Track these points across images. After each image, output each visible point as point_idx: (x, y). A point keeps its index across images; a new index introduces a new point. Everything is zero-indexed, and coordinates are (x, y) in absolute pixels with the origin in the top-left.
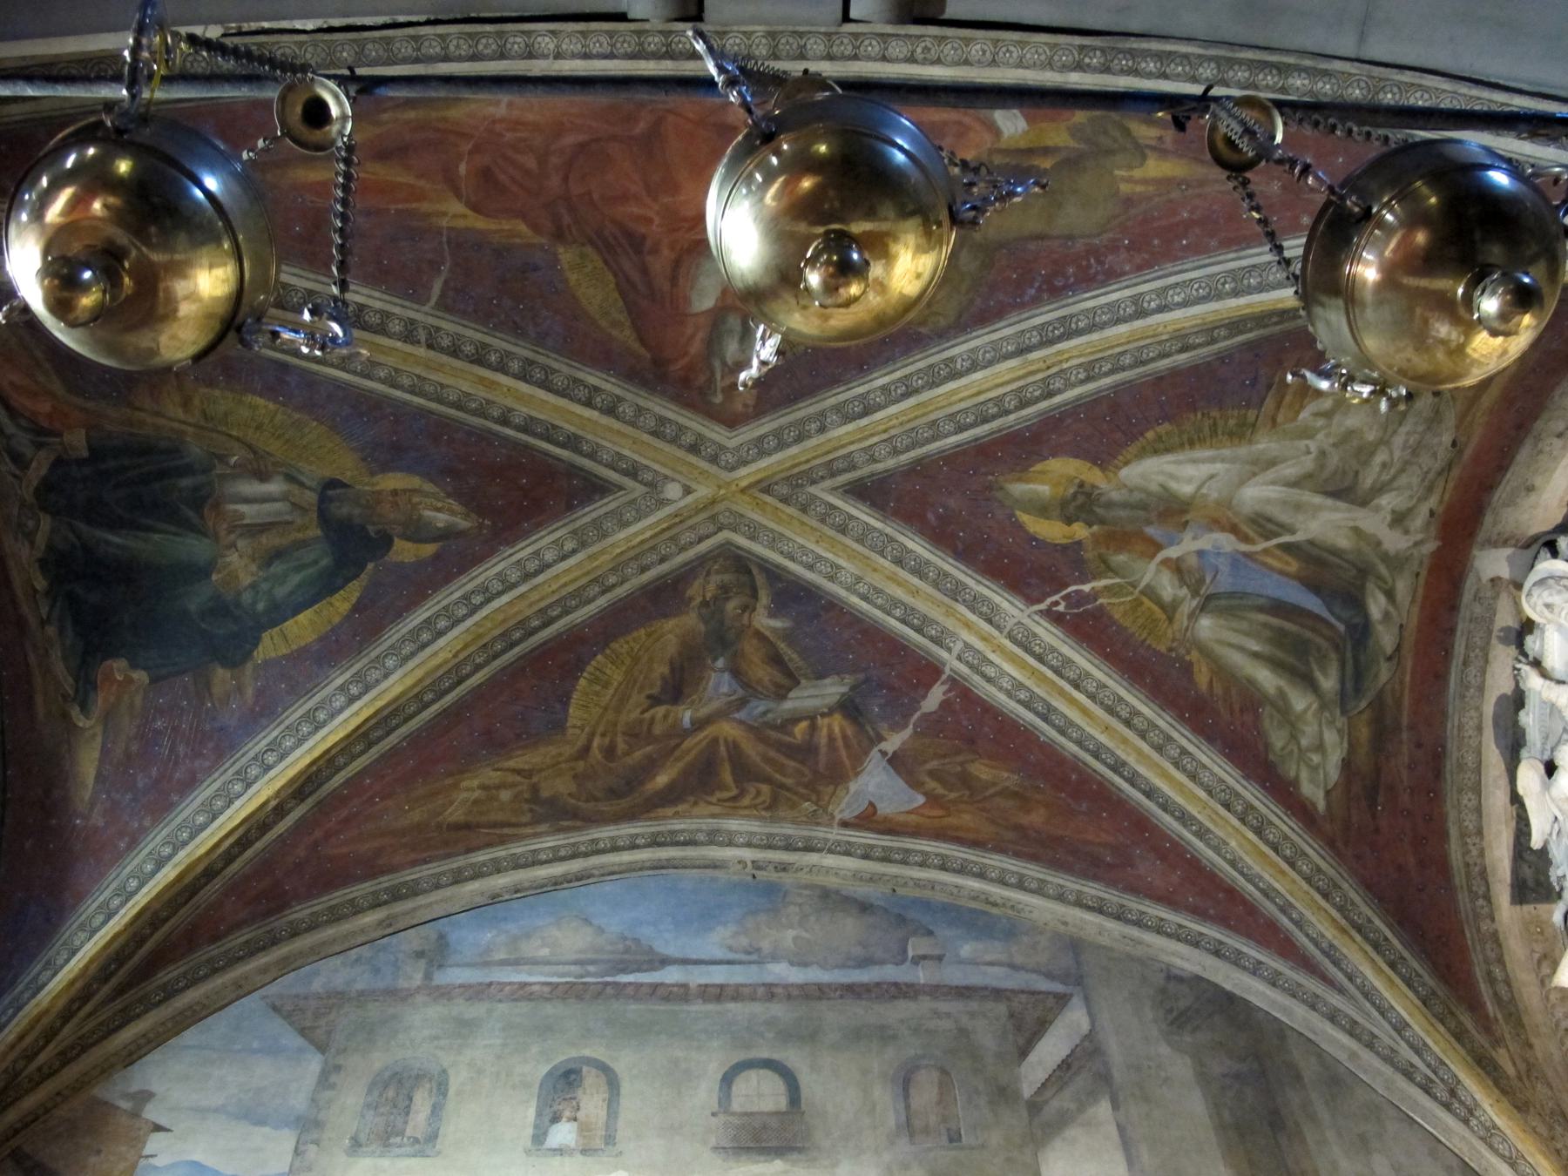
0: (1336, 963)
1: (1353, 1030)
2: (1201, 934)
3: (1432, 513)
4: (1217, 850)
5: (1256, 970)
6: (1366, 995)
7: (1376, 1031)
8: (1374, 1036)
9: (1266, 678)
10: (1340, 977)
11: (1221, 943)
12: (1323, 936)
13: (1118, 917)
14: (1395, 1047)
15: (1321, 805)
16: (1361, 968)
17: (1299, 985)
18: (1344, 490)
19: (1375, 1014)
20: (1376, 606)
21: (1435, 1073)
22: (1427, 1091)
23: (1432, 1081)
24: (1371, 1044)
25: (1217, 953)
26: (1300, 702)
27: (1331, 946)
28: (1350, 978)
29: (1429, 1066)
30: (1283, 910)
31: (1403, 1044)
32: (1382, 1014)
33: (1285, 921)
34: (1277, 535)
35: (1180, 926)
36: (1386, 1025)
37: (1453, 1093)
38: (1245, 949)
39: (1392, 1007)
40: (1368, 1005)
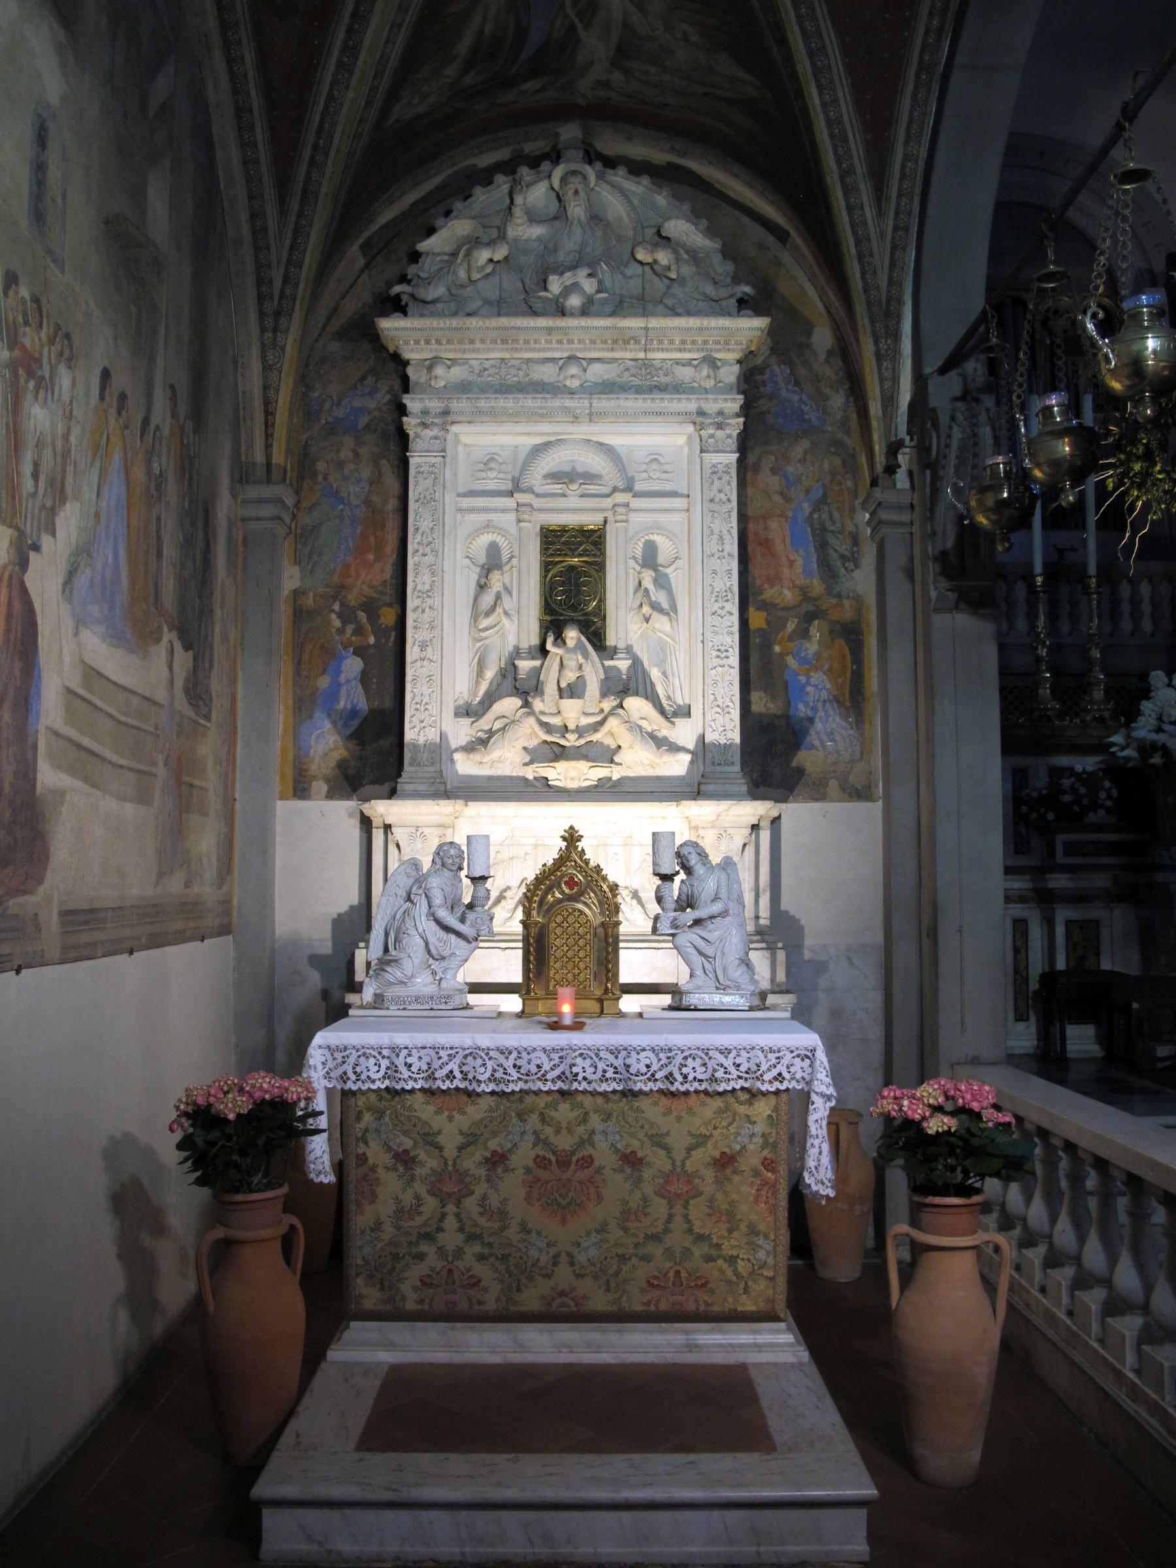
0: (303, 201)
1: (259, 233)
2: (248, 93)
3: (609, 99)
4: (335, 82)
5: (246, 145)
6: (296, 232)
7: (273, 248)
8: (268, 247)
9: (465, 45)
10: (294, 205)
11: (251, 111)
13: (224, 26)
15: (391, 121)
16: (315, 221)
17: (260, 181)
18: (622, 54)
19: (287, 243)
20: (531, 85)
21: (281, 298)
22: (261, 298)
23: (272, 298)
24: (260, 248)
25: (238, 112)
26: (451, 71)
28: (300, 215)
29: (282, 292)
30: (315, 148)
31: (282, 270)
33: (307, 152)
34: (581, 21)
35: (245, 76)
37: (277, 315)
38: (258, 130)
39: (304, 253)
40: (290, 234)
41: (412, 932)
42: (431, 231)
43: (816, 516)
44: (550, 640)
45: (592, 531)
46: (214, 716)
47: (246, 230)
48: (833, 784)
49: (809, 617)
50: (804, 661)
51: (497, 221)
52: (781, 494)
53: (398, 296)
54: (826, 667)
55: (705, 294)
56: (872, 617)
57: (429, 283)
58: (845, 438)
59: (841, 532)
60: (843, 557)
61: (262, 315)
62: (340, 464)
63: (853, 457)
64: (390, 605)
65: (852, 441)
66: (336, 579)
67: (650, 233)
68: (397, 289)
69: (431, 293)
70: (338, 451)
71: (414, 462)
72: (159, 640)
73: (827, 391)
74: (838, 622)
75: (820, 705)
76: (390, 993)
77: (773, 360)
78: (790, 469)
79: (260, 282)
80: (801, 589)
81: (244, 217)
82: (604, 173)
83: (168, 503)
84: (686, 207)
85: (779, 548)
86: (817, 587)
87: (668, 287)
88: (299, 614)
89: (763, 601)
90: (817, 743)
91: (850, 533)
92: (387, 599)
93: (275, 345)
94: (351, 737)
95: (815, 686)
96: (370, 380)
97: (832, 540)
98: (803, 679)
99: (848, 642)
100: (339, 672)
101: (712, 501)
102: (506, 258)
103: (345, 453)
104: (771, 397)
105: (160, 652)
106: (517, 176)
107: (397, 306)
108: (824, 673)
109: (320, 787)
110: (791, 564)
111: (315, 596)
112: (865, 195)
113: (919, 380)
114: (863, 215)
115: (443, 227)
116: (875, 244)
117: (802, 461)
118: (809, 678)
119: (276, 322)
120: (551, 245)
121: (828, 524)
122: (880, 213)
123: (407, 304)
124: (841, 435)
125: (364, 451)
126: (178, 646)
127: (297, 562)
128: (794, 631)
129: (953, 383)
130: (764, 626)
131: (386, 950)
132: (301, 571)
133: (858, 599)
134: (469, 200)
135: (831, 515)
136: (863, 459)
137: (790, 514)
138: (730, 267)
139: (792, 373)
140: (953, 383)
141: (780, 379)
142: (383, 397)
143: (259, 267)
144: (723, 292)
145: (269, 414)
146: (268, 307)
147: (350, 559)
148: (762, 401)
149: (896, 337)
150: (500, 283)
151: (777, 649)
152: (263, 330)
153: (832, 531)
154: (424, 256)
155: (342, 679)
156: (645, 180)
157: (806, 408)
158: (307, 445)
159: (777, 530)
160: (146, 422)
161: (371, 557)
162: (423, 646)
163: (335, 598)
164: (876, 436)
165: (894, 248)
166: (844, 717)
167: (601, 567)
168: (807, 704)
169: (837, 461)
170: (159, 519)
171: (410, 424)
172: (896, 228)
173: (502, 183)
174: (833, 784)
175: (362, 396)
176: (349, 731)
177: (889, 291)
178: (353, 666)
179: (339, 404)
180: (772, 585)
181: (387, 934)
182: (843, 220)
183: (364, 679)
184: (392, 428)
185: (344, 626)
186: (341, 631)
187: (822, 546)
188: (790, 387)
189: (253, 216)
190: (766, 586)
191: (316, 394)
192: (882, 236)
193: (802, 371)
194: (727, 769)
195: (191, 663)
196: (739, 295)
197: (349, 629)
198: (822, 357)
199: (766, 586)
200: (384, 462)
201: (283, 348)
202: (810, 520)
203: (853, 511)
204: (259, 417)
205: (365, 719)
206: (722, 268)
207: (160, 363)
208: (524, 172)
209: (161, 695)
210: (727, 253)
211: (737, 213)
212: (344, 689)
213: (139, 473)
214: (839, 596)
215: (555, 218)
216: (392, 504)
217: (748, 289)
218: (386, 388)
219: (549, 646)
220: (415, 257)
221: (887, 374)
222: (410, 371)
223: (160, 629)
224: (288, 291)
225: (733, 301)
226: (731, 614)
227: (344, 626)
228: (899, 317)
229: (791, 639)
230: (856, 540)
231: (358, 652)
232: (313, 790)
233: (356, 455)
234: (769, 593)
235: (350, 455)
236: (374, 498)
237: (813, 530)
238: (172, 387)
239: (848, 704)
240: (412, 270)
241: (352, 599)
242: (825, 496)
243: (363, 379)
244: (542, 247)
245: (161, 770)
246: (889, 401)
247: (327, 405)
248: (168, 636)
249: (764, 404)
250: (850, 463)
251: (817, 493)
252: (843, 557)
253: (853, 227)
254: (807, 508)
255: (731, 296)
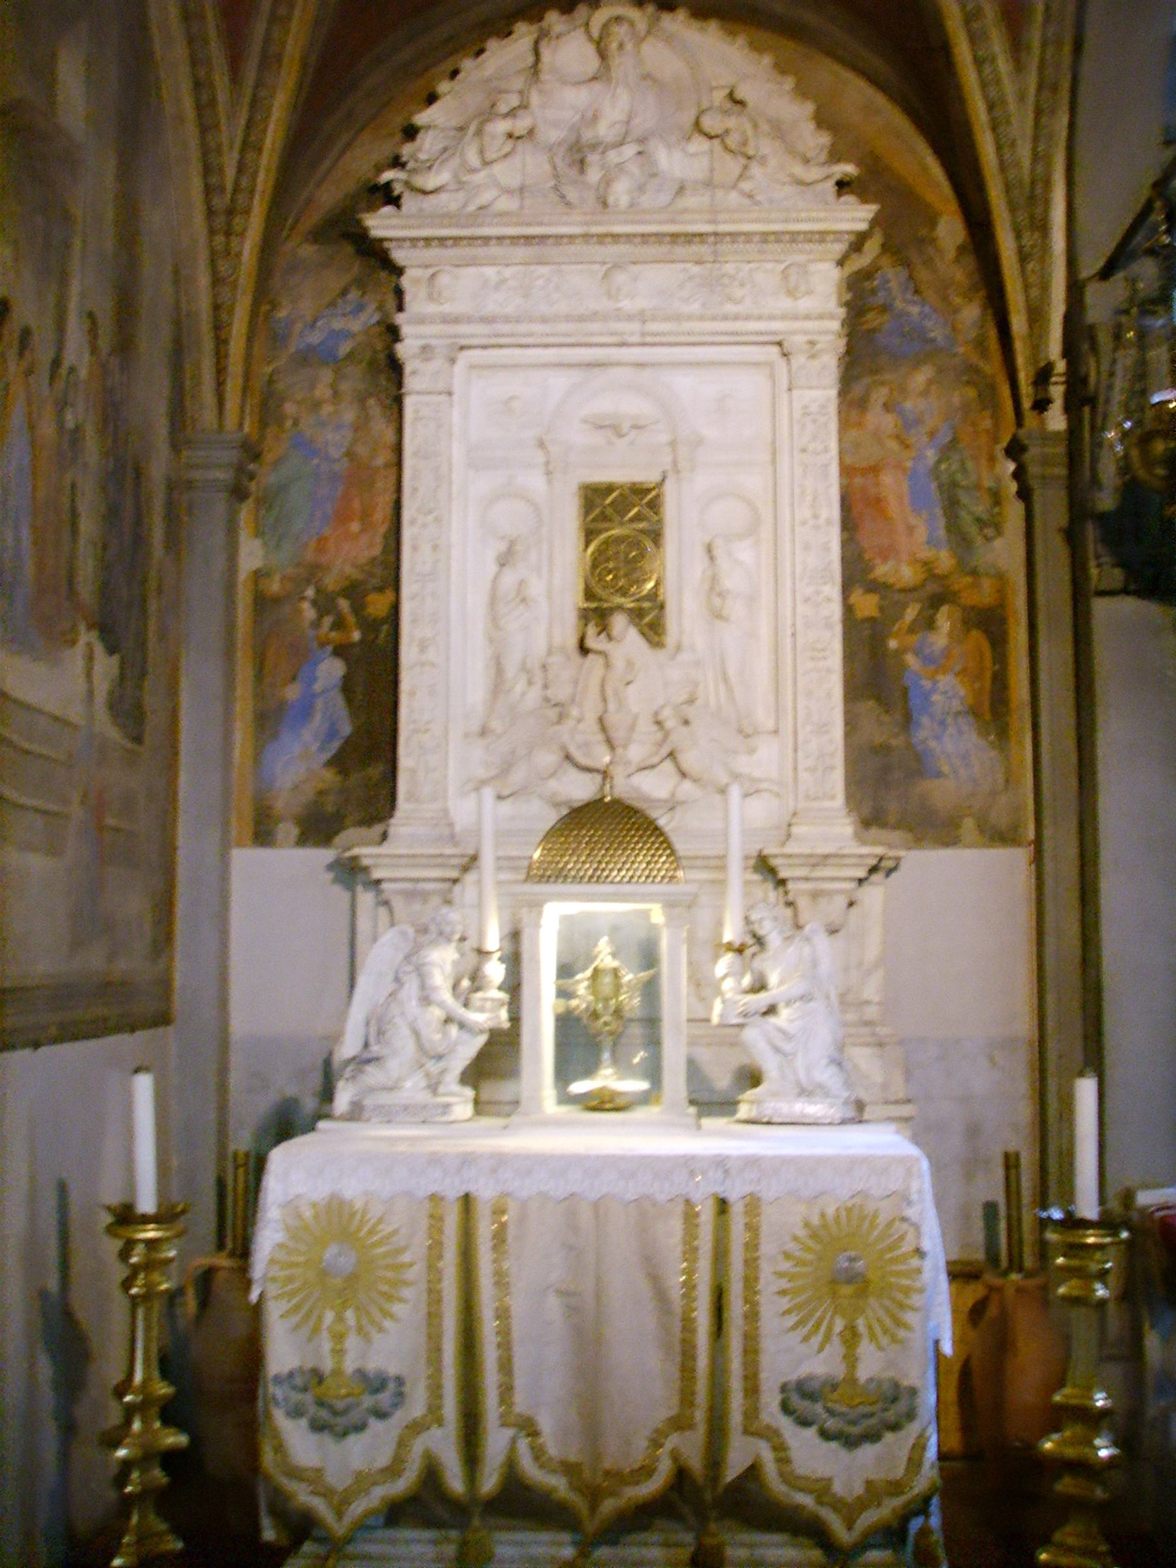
1: (205, 108)
8: (217, 126)
10: (250, 74)
12: (283, 44)
14: (225, 149)
21: (236, 190)
22: (208, 190)
27: (279, 58)
28: (258, 85)
29: (237, 183)
31: (236, 155)
32: (249, 125)
36: (240, 134)
37: (230, 212)
41: (398, 1020)
42: (432, 99)
43: (943, 467)
44: (591, 630)
45: (649, 490)
46: (147, 739)
47: (188, 104)
48: (969, 824)
49: (936, 601)
50: (928, 660)
51: (518, 83)
52: (897, 437)
53: (388, 185)
54: (958, 668)
55: (791, 175)
56: (1019, 602)
57: (430, 168)
58: (981, 364)
59: (978, 487)
60: (979, 520)
61: (210, 213)
62: (316, 405)
63: (993, 387)
64: (380, 589)
65: (993, 367)
66: (309, 555)
67: (719, 96)
68: (388, 176)
69: (431, 181)
70: (312, 387)
71: (409, 403)
72: (73, 643)
73: (958, 300)
74: (973, 608)
75: (949, 720)
76: (368, 1102)
77: (885, 261)
78: (908, 405)
79: (207, 170)
80: (925, 564)
81: (186, 86)
82: (658, 19)
83: (86, 465)
84: (767, 60)
85: (893, 508)
86: (945, 560)
87: (746, 167)
88: (262, 603)
89: (874, 581)
90: (946, 769)
91: (990, 489)
92: (375, 582)
93: (228, 252)
94: (330, 763)
95: (945, 693)
96: (354, 295)
97: (964, 499)
98: (926, 684)
99: (987, 632)
100: (313, 679)
101: (804, 450)
102: (531, 132)
103: (322, 391)
104: (885, 308)
105: (75, 658)
106: (544, 24)
107: (388, 197)
108: (956, 675)
109: (288, 830)
110: (910, 530)
111: (282, 580)
112: (997, 44)
113: (1075, 289)
114: (995, 71)
115: (445, 94)
116: (1012, 106)
117: (925, 393)
118: (935, 683)
119: (229, 223)
120: (590, 114)
121: (959, 477)
122: (1019, 66)
123: (399, 197)
124: (975, 359)
125: (345, 387)
126: (99, 649)
127: (258, 533)
128: (914, 620)
129: (1116, 290)
130: (875, 613)
131: (366, 1045)
132: (265, 544)
133: (1001, 578)
134: (484, 56)
135: (963, 463)
136: (1005, 391)
137: (909, 464)
138: (825, 139)
139: (911, 277)
140: (1116, 290)
141: (893, 285)
142: (370, 316)
143: (205, 152)
144: (814, 173)
145: (221, 343)
146: (219, 203)
147: (327, 531)
148: (870, 316)
149: (1043, 227)
150: (524, 166)
151: (893, 644)
152: (212, 232)
153: (963, 487)
154: (422, 131)
155: (318, 687)
156: (713, 26)
157: (929, 324)
158: (271, 382)
159: (892, 485)
160: (56, 363)
161: (355, 527)
162: (423, 648)
163: (308, 581)
164: (1020, 360)
165: (1038, 113)
166: (983, 732)
167: (656, 536)
168: (932, 717)
169: (971, 393)
170: (73, 486)
171: (403, 350)
172: (1040, 87)
173: (524, 33)
174: (969, 824)
175: (344, 315)
176: (327, 756)
177: (1033, 171)
178: (331, 670)
179: (313, 325)
180: (885, 559)
181: (368, 1024)
182: (969, 77)
183: (347, 687)
184: (382, 356)
185: (320, 617)
186: (316, 624)
187: (952, 505)
188: (909, 296)
189: (198, 85)
190: (878, 561)
191: (282, 314)
192: (1022, 98)
193: (923, 274)
194: (827, 804)
195: (115, 671)
196: (838, 177)
197: (327, 621)
198: (951, 254)
199: (878, 561)
200: (372, 402)
201: (238, 255)
202: (935, 472)
203: (992, 459)
204: (208, 344)
205: (348, 741)
206: (816, 141)
207: (75, 288)
208: (553, 18)
209: (75, 713)
210: (822, 121)
211: (837, 67)
212: (319, 704)
213: (47, 429)
214: (974, 573)
215: (594, 78)
216: (383, 458)
217: (848, 169)
218: (374, 306)
219: (591, 643)
220: (411, 132)
221: (1033, 279)
222: (405, 282)
223: (74, 628)
224: (244, 182)
225: (830, 186)
226: (829, 600)
227: (320, 617)
228: (1047, 203)
229: (912, 630)
230: (996, 497)
231: (340, 651)
232: (280, 836)
233: (336, 394)
234: (882, 570)
235: (328, 393)
236: (362, 450)
237: (940, 486)
238: (91, 315)
239: (988, 717)
240: (407, 150)
241: (331, 582)
242: (954, 441)
243: (344, 293)
244: (578, 117)
245: (76, 811)
246: (1037, 316)
247: (299, 326)
248: (87, 637)
249: (872, 319)
250: (988, 398)
251: (945, 438)
252: (981, 523)
253: (984, 85)
254: (931, 455)
255: (828, 177)
